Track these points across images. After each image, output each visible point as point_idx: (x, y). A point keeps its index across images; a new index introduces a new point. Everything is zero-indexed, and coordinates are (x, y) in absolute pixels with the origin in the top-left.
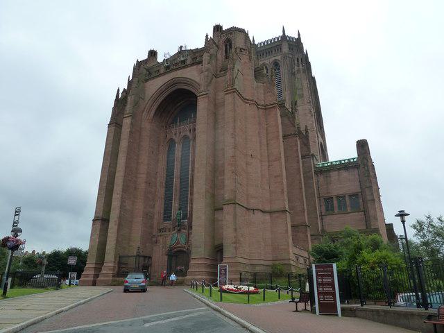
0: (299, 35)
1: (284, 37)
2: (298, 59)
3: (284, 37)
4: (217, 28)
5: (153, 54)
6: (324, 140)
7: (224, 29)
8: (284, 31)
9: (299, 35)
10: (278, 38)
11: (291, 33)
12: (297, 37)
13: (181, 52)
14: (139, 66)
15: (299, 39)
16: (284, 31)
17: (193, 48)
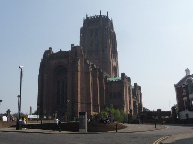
0: (108, 14)
1: (101, 15)
2: (106, 29)
3: (101, 15)
4: (73, 45)
5: (50, 49)
6: (117, 62)
7: (75, 46)
8: (101, 13)
9: (108, 14)
10: (98, 16)
11: (104, 14)
12: (106, 15)
13: (61, 52)
14: (46, 52)
15: (107, 16)
16: (101, 13)
17: (65, 51)
